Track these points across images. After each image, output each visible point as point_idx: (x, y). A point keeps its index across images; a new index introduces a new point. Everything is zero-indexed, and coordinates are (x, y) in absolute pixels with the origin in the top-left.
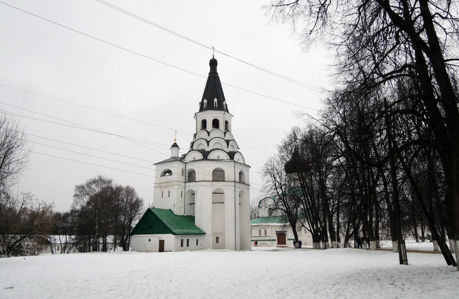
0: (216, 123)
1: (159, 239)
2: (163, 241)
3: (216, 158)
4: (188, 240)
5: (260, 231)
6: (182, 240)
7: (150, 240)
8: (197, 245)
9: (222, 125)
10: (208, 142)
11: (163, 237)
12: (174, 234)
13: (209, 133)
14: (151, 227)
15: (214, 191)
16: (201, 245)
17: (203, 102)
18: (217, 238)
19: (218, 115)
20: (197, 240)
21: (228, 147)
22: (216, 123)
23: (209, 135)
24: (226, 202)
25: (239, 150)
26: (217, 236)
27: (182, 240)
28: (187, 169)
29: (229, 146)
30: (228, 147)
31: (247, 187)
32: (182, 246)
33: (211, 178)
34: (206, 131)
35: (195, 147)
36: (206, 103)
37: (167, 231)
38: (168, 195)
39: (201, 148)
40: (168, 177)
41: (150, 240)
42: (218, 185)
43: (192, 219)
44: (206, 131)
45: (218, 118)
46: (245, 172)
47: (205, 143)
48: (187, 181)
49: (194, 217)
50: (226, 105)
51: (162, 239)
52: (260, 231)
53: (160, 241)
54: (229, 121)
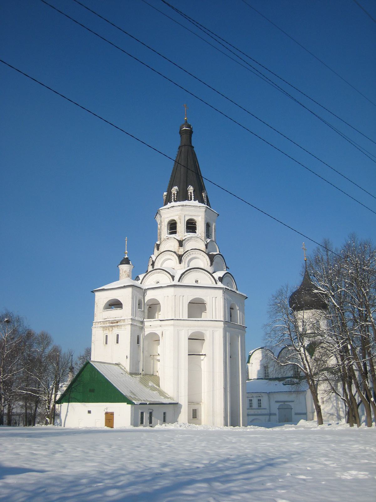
0: (191, 226)
2: (112, 414)
4: (151, 414)
5: (251, 400)
7: (89, 412)
10: (180, 257)
13: (181, 243)
14: (92, 391)
17: (171, 193)
20: (164, 413)
27: (142, 413)
40: (115, 313)
41: (89, 412)
42: (194, 326)
51: (109, 411)
52: (251, 400)
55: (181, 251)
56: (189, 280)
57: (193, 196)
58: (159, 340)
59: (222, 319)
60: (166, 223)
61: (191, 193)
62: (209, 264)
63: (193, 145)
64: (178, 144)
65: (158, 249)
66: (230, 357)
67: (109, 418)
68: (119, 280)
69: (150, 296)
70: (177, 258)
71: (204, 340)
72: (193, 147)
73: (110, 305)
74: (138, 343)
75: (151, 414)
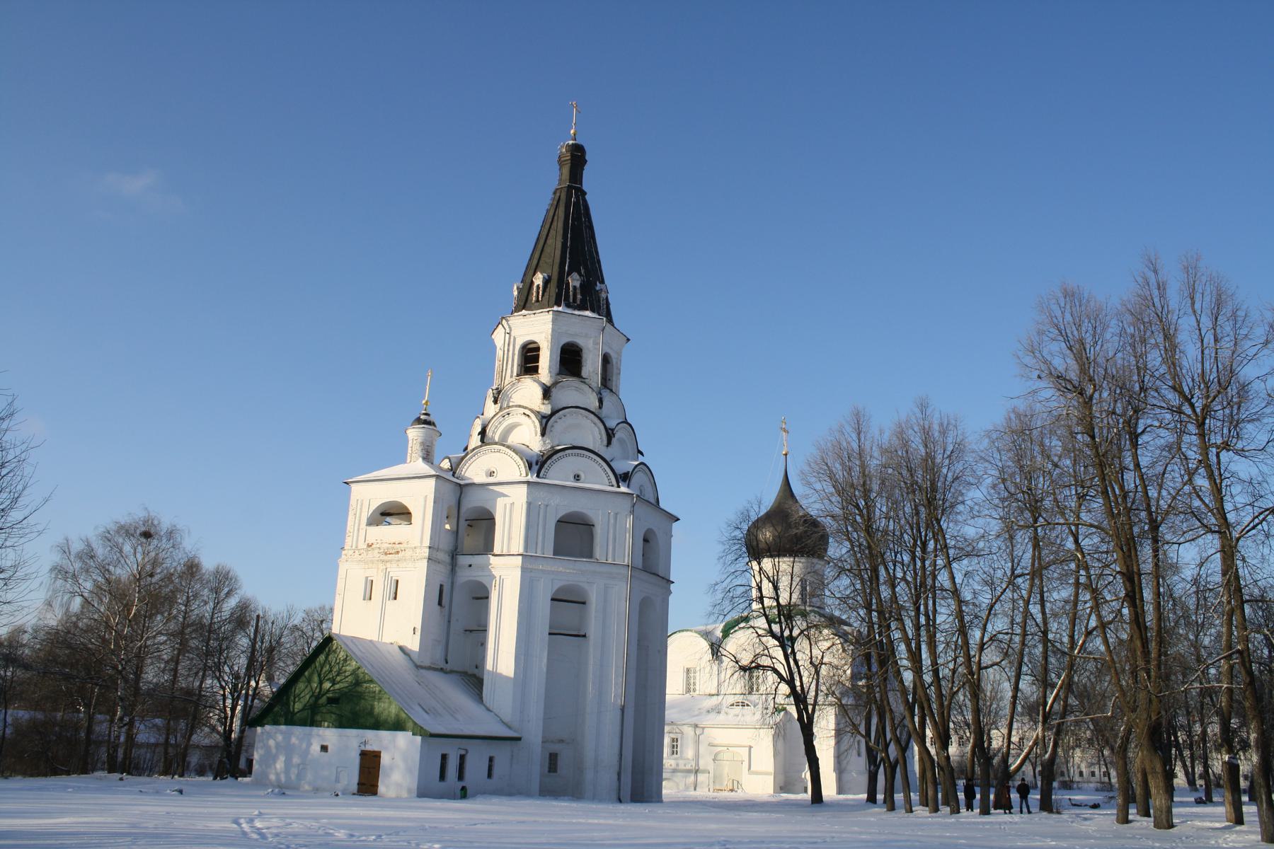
2: (376, 756)
6: (444, 757)
8: (490, 775)
9: (592, 366)
12: (418, 730)
15: (558, 591)
17: (532, 283)
20: (491, 759)
21: (609, 443)
22: (570, 359)
26: (555, 748)
27: (444, 757)
28: (463, 509)
29: (614, 440)
30: (609, 443)
32: (442, 777)
38: (392, 595)
39: (513, 439)
45: (580, 342)
53: (364, 754)
54: (613, 355)
60: (518, 347)
63: (584, 188)
64: (555, 184)
68: (405, 462)
71: (584, 603)
72: (584, 193)
74: (440, 603)
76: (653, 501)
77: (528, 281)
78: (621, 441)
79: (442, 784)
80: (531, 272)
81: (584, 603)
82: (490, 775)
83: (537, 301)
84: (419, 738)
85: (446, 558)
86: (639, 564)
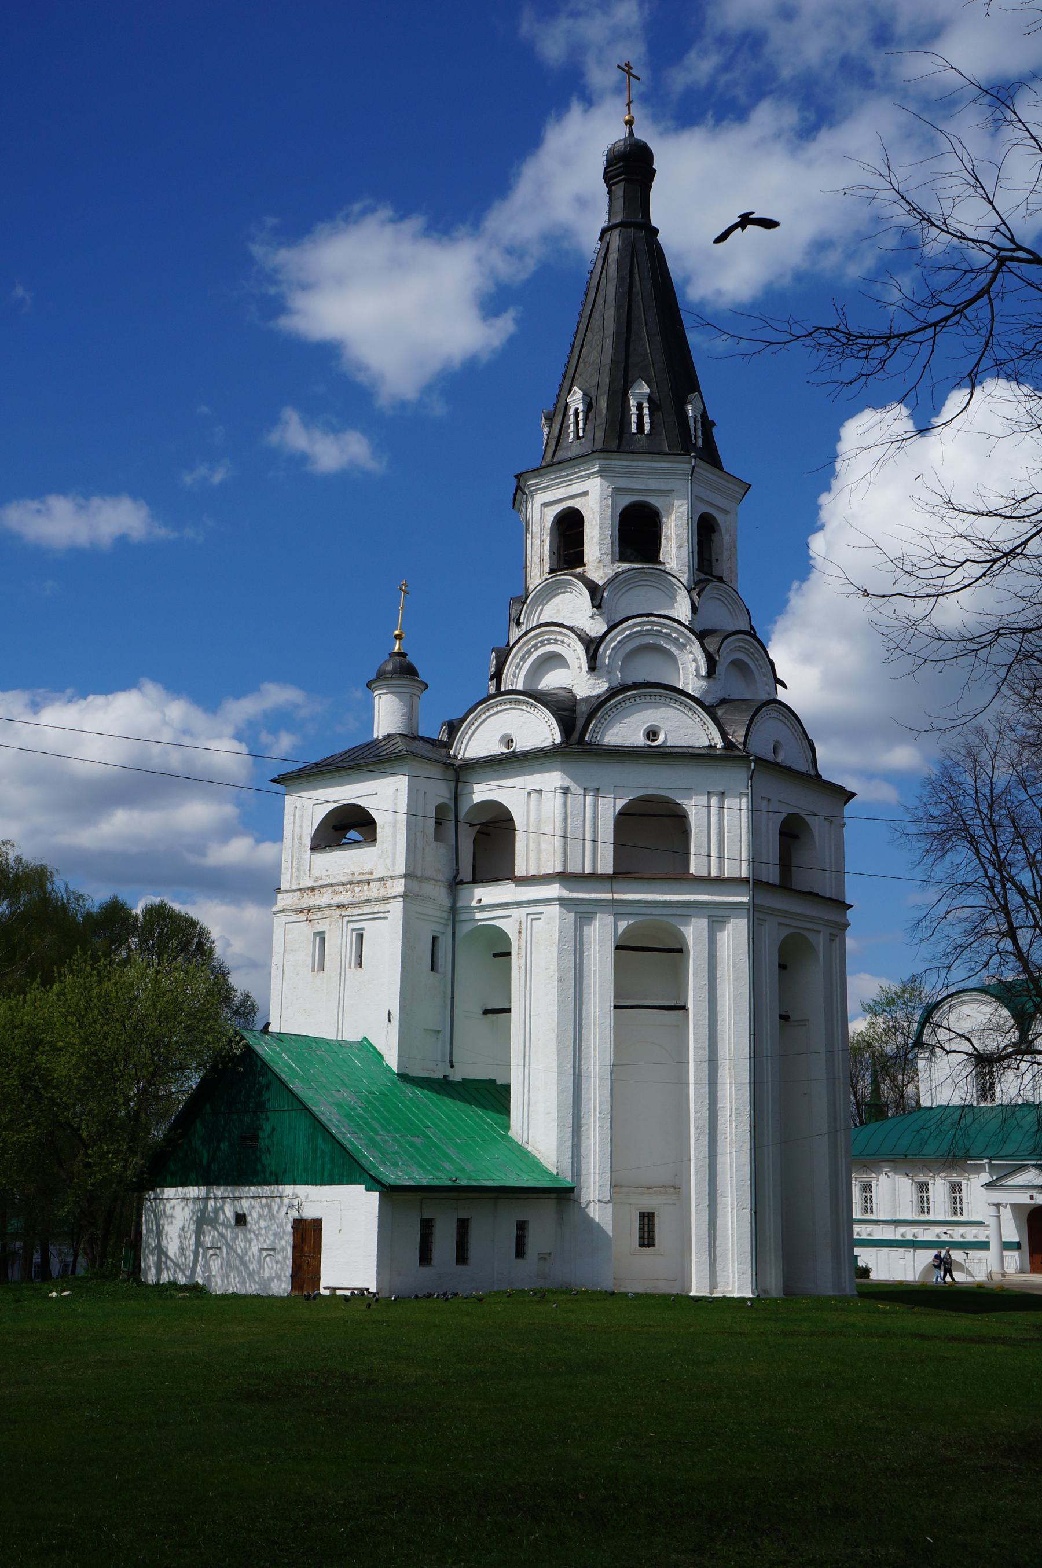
1: (294, 1214)
3: (639, 739)
4: (463, 1226)
8: (520, 1253)
10: (592, 646)
11: (315, 1200)
12: (373, 1183)
16: (543, 1258)
17: (567, 406)
18: (647, 1221)
19: (653, 484)
22: (637, 532)
23: (597, 604)
24: (690, 1005)
25: (782, 694)
26: (648, 1203)
29: (720, 669)
31: (832, 915)
32: (425, 1258)
33: (606, 865)
34: (582, 578)
35: (515, 678)
36: (581, 407)
37: (341, 1167)
39: (552, 681)
43: (494, 1096)
44: (582, 578)
46: (816, 824)
47: (575, 653)
48: (466, 873)
49: (507, 1088)
50: (708, 425)
55: (596, 628)
56: (626, 731)
57: (647, 419)
58: (509, 954)
59: (744, 874)
60: (548, 524)
61: (640, 407)
62: (703, 672)
65: (518, 624)
66: (784, 1018)
67: (307, 1235)
69: (482, 792)
70: (580, 649)
72: (656, 231)
73: (336, 828)
75: (463, 1226)
76: (803, 766)
77: (562, 403)
78: (738, 665)
79: (425, 1270)
80: (567, 383)
81: (680, 951)
82: (520, 1253)
83: (578, 437)
84: (375, 1195)
85: (440, 894)
86: (773, 875)
